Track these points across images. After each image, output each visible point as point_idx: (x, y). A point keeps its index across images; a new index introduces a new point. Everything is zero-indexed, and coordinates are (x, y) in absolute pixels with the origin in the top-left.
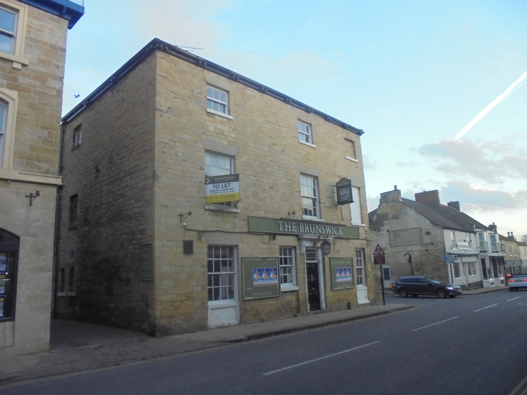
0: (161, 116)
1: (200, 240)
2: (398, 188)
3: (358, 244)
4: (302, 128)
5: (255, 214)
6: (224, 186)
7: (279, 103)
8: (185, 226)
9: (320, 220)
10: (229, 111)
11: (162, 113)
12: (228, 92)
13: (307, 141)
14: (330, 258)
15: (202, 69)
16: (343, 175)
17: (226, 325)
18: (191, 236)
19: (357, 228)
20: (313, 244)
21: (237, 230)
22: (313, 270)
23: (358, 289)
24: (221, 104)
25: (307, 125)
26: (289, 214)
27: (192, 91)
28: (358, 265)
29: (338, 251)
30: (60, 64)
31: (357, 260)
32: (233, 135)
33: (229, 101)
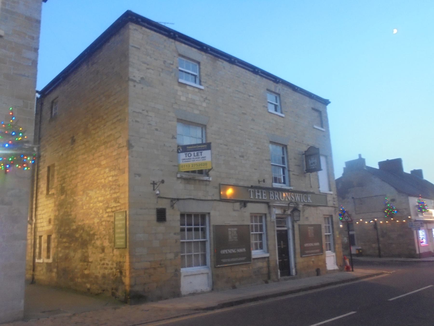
0: (135, 86)
1: (173, 208)
2: (363, 157)
3: (326, 211)
4: (271, 98)
6: (196, 155)
7: (249, 75)
8: (157, 194)
9: (288, 188)
10: (200, 81)
11: (136, 84)
12: (199, 63)
13: (276, 110)
14: (299, 225)
15: (173, 41)
16: (311, 143)
17: (199, 291)
18: (164, 204)
19: (325, 195)
20: (283, 211)
21: (209, 198)
22: (283, 237)
23: (327, 255)
24: (192, 75)
25: (276, 95)
26: (259, 182)
27: (165, 62)
28: (326, 233)
29: (307, 218)
30: (35, 36)
31: (326, 226)
32: (204, 105)
33: (200, 72)
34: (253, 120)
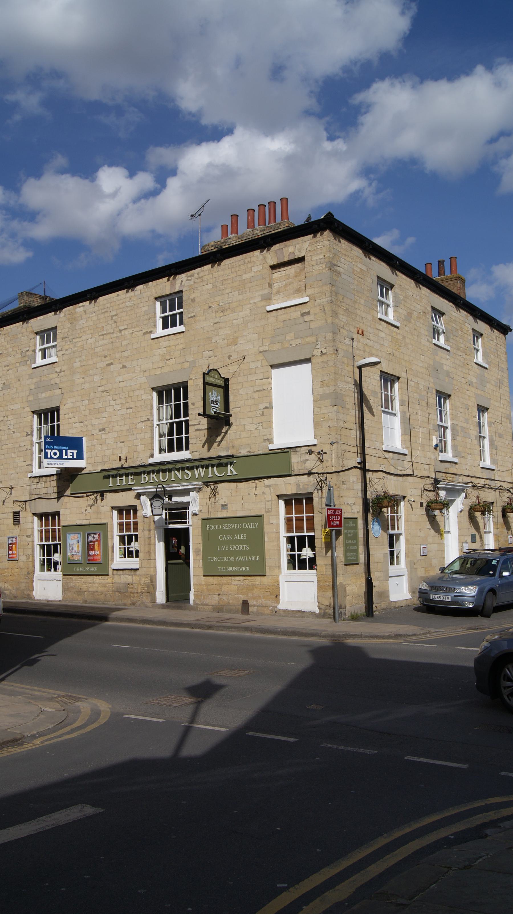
29: (226, 505)
34: (124, 367)
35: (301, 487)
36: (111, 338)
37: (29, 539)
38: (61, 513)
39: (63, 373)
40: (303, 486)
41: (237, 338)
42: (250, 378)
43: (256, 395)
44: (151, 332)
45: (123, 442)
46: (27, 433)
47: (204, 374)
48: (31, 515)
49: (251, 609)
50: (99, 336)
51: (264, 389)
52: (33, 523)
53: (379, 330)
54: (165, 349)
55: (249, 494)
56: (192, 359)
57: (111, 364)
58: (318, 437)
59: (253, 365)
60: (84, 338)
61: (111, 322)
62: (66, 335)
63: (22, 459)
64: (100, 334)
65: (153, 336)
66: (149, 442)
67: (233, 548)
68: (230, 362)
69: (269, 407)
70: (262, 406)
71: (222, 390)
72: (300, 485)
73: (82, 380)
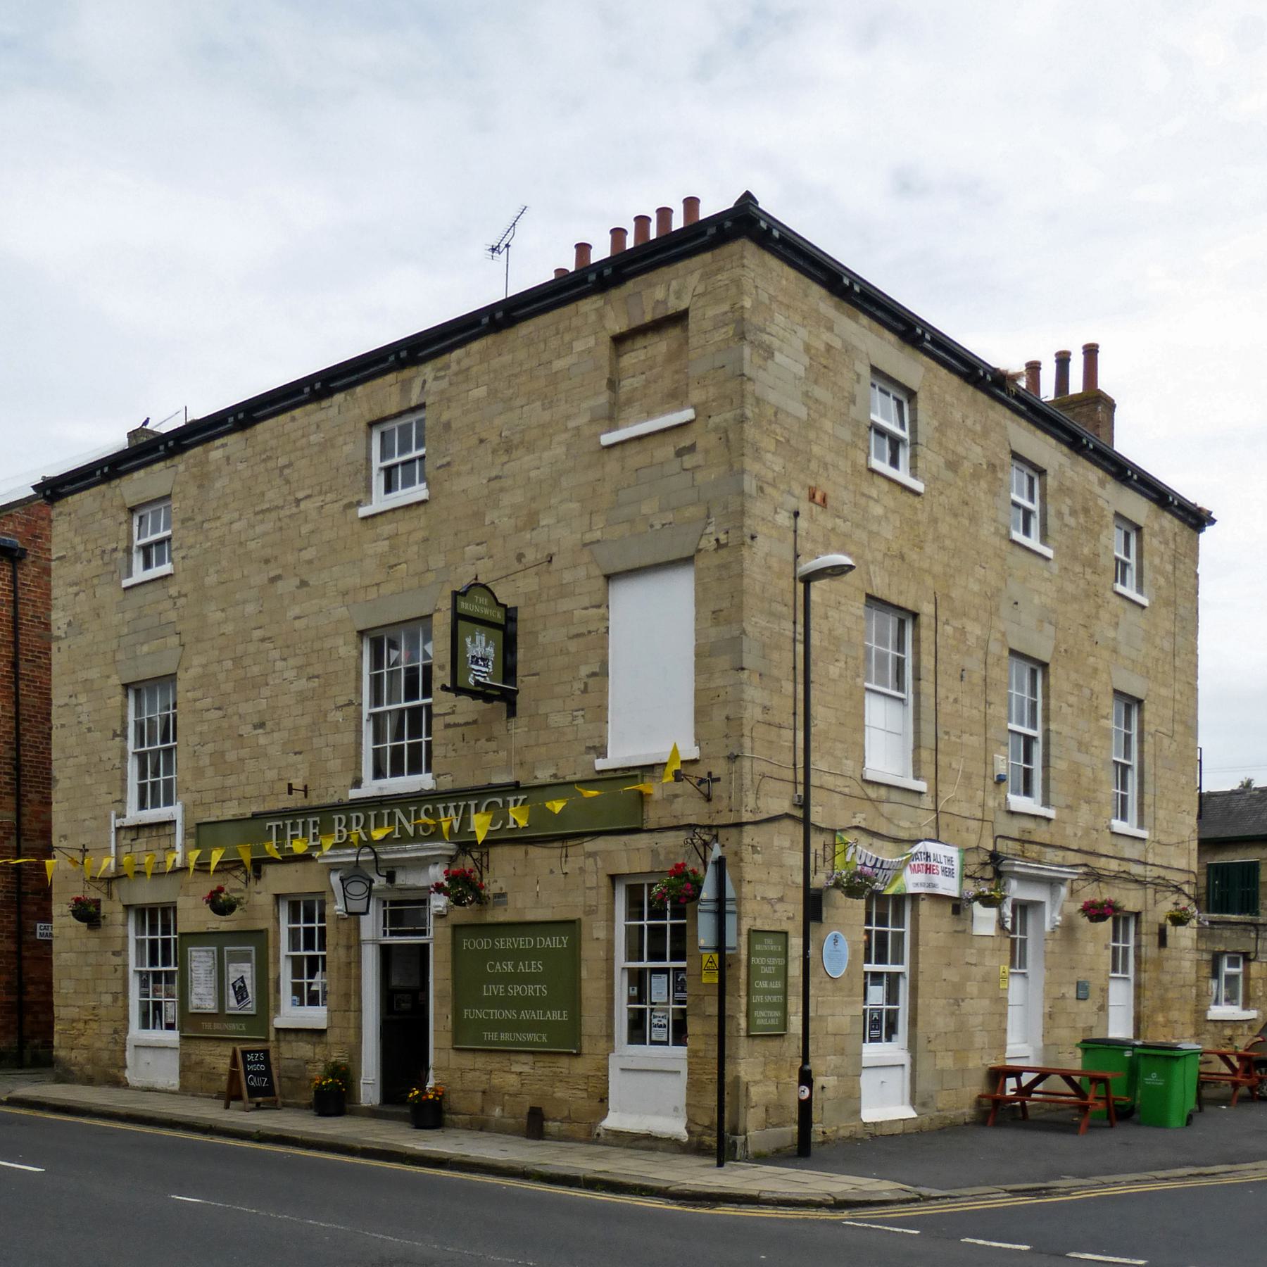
3: (634, 855)
5: (215, 814)
35: (662, 857)
36: (280, 519)
37: (118, 960)
38: (179, 906)
39: (182, 601)
40: (668, 853)
41: (537, 513)
42: (564, 605)
43: (573, 646)
44: (359, 504)
45: (300, 753)
46: (115, 732)
47: (456, 594)
48: (120, 908)
49: (551, 1126)
50: (256, 514)
51: (590, 632)
52: (125, 925)
53: (870, 497)
54: (387, 542)
55: (552, 872)
56: (441, 564)
57: (278, 578)
58: (703, 744)
59: (568, 577)
60: (226, 518)
61: (278, 482)
62: (189, 514)
63: (104, 789)
64: (258, 509)
65: (363, 511)
66: (353, 753)
67: (515, 990)
68: (521, 567)
69: (602, 673)
70: (584, 671)
71: (499, 634)
72: (659, 854)
73: (219, 615)
